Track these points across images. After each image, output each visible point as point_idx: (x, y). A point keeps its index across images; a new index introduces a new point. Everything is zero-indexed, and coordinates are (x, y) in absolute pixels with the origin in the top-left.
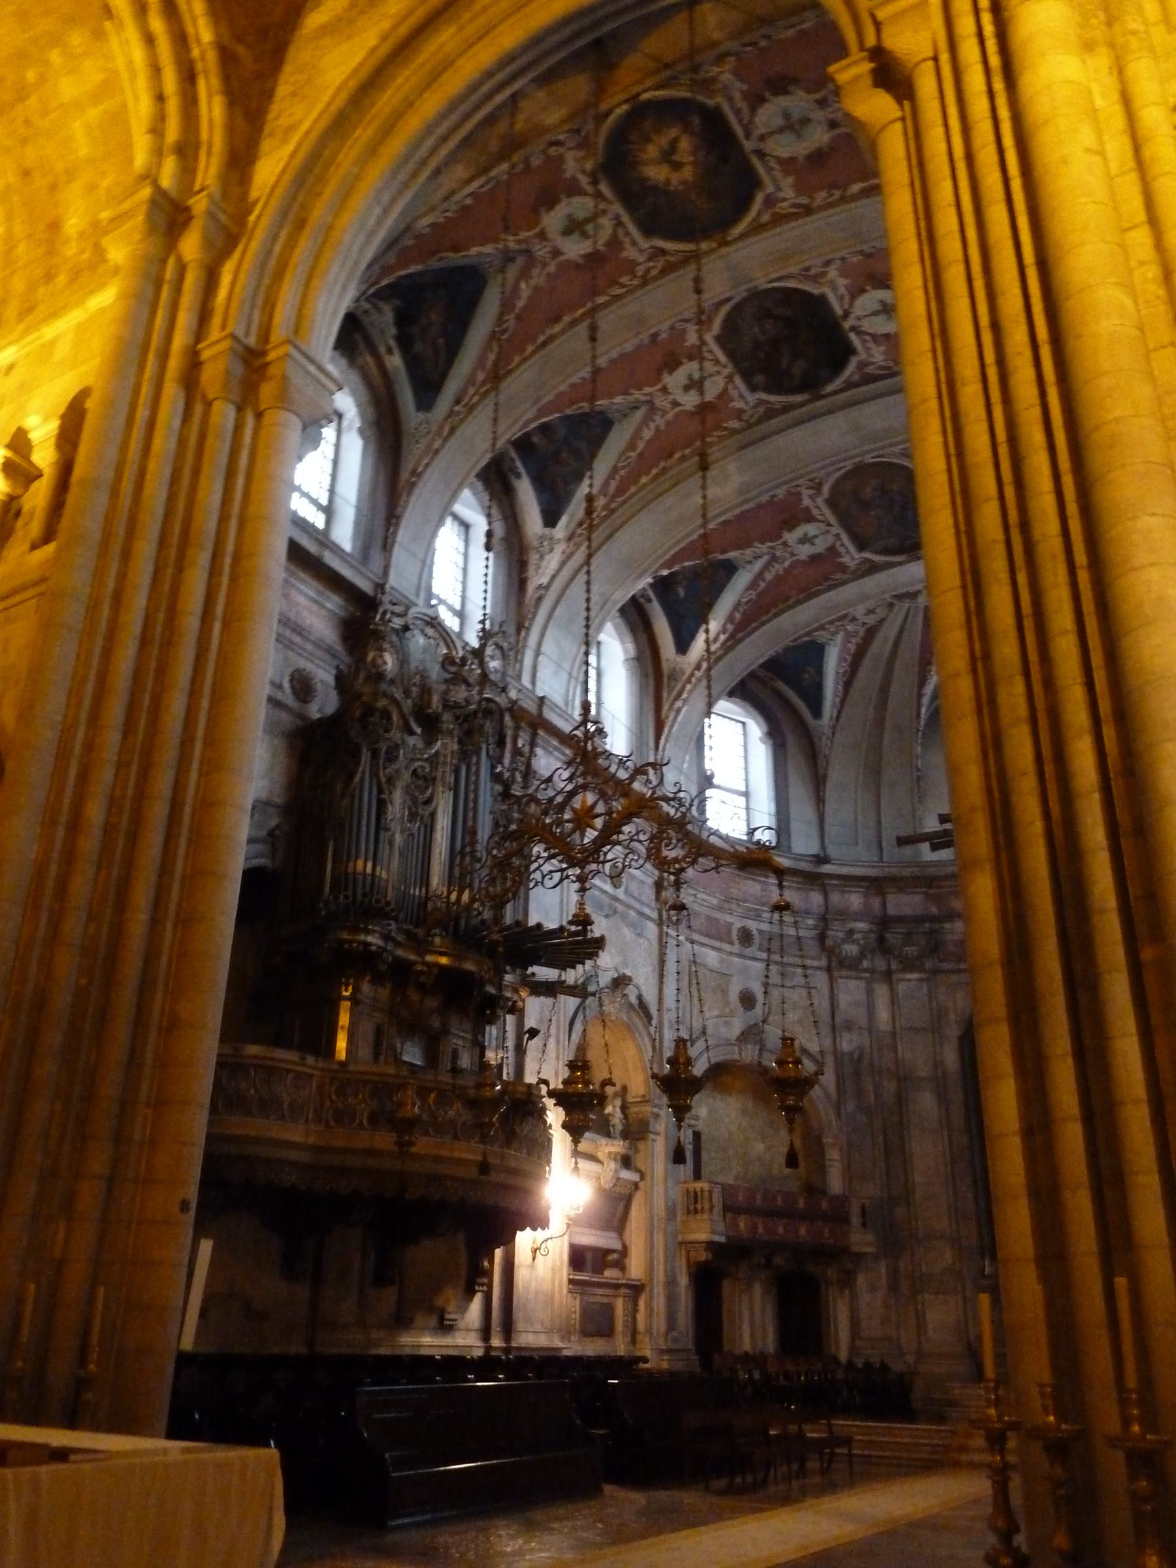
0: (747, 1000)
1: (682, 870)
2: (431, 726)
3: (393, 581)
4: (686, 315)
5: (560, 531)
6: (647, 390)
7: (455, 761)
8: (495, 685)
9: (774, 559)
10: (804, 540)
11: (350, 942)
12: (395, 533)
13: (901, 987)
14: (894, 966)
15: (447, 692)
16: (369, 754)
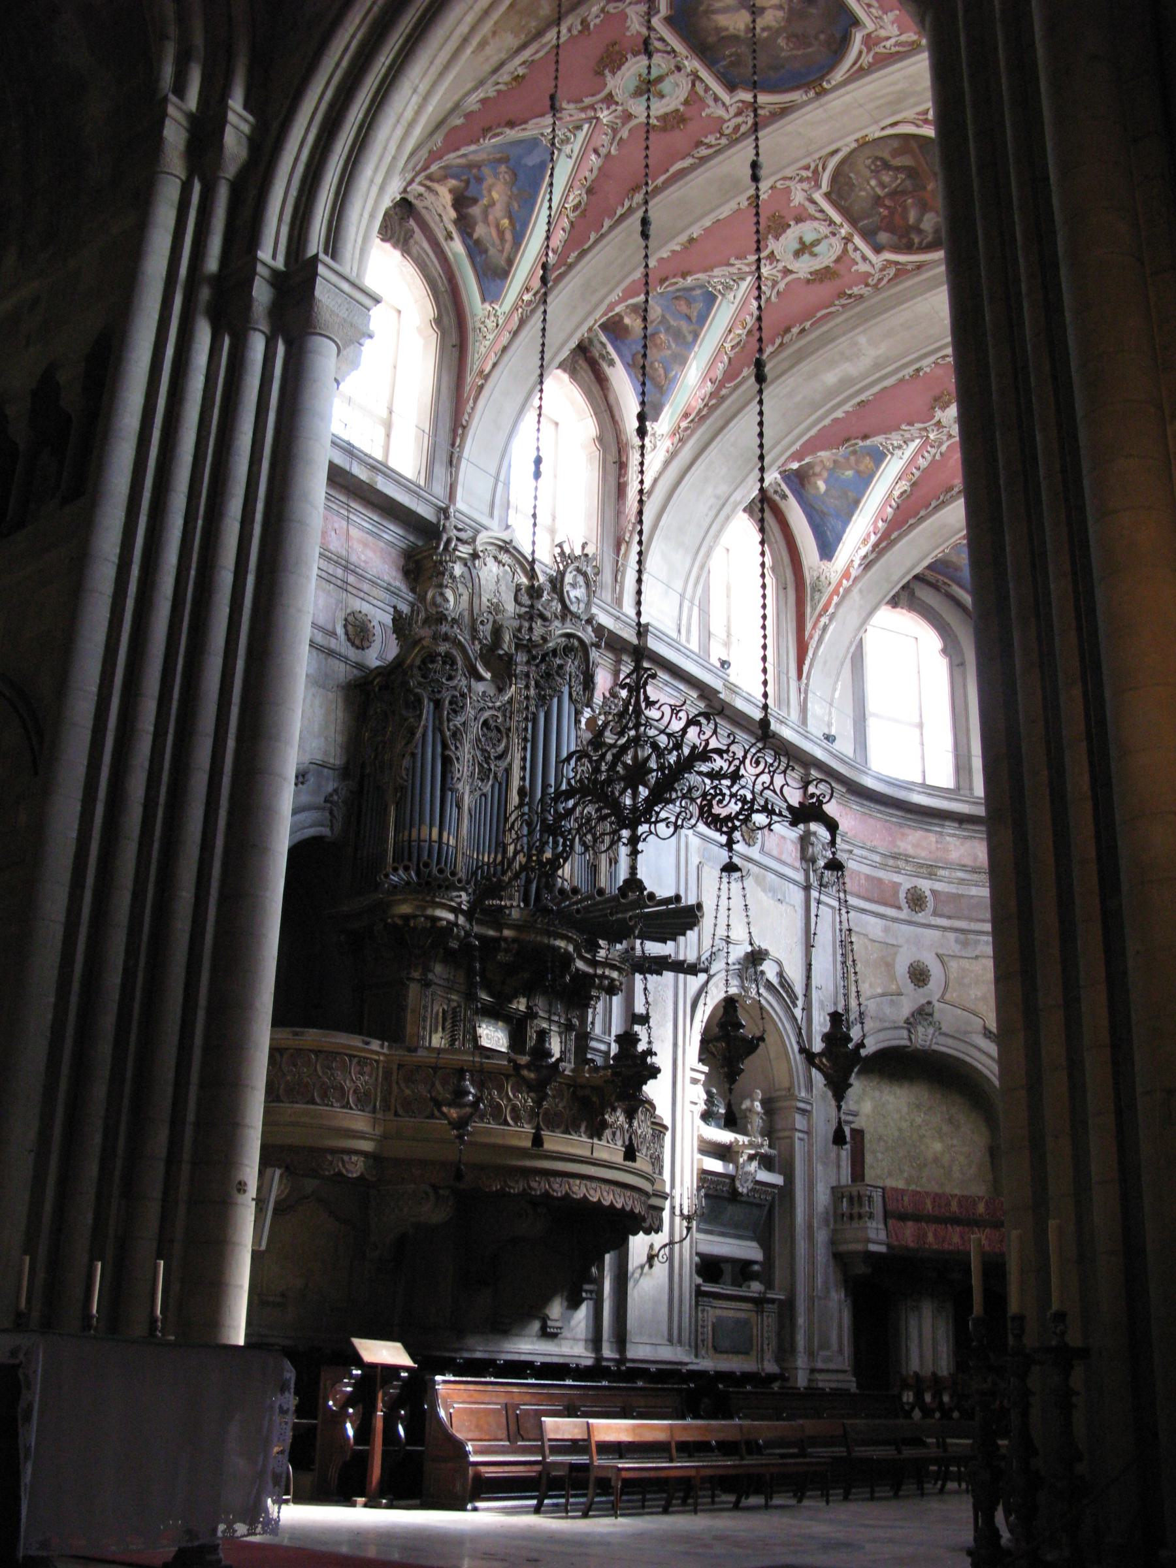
0: (919, 976)
1: (735, 828)
2: (503, 671)
3: (460, 504)
4: (788, 172)
7: (533, 709)
8: (578, 618)
11: (415, 917)
12: (461, 446)
16: (432, 705)
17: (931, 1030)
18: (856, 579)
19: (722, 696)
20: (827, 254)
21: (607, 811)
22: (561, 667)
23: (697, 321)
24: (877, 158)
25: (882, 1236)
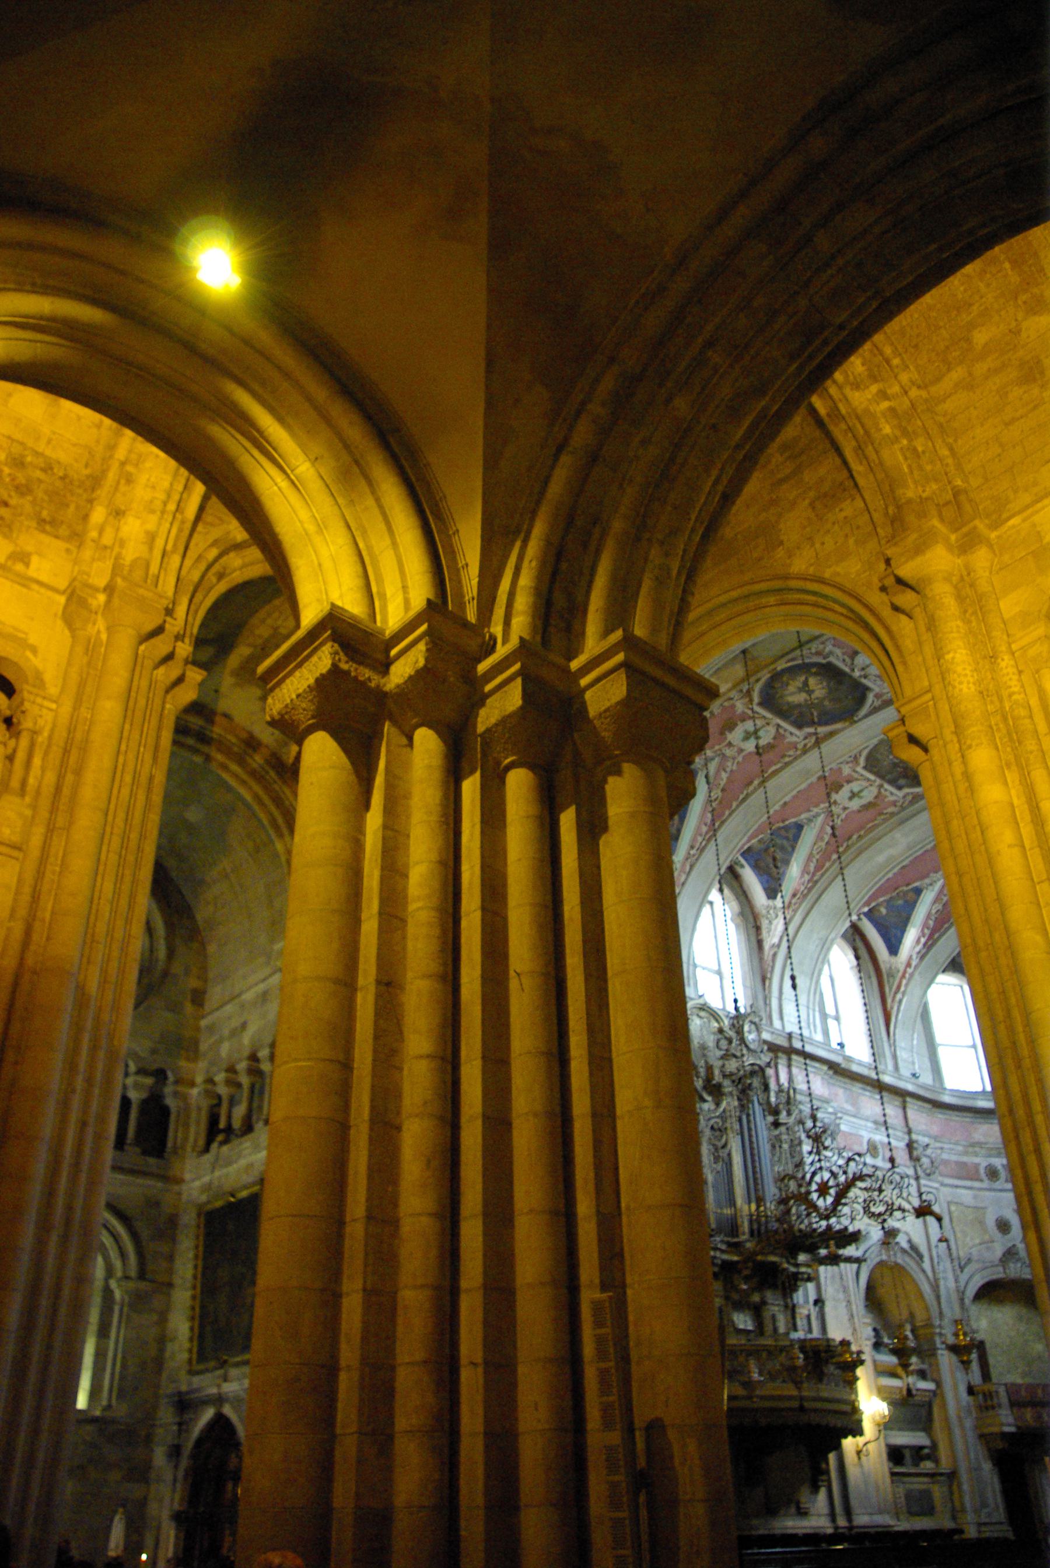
1: (885, 1220)
15: (723, 1066)
17: (1019, 1265)
18: (916, 967)
19: (843, 1066)
20: (869, 795)
22: (750, 1085)
25: (1011, 1420)
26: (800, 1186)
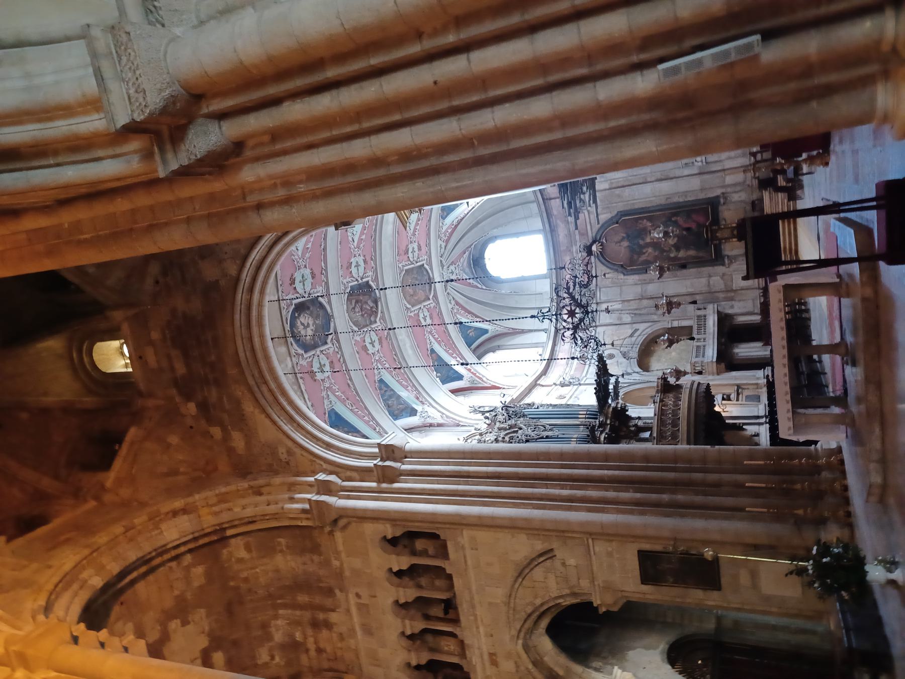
5: (419, 408)
6: (373, 360)
7: (528, 419)
9: (430, 332)
10: (425, 319)
13: (603, 298)
14: (594, 302)
17: (631, 352)
21: (582, 324)
23: (388, 388)
24: (351, 310)
26: (568, 329)
